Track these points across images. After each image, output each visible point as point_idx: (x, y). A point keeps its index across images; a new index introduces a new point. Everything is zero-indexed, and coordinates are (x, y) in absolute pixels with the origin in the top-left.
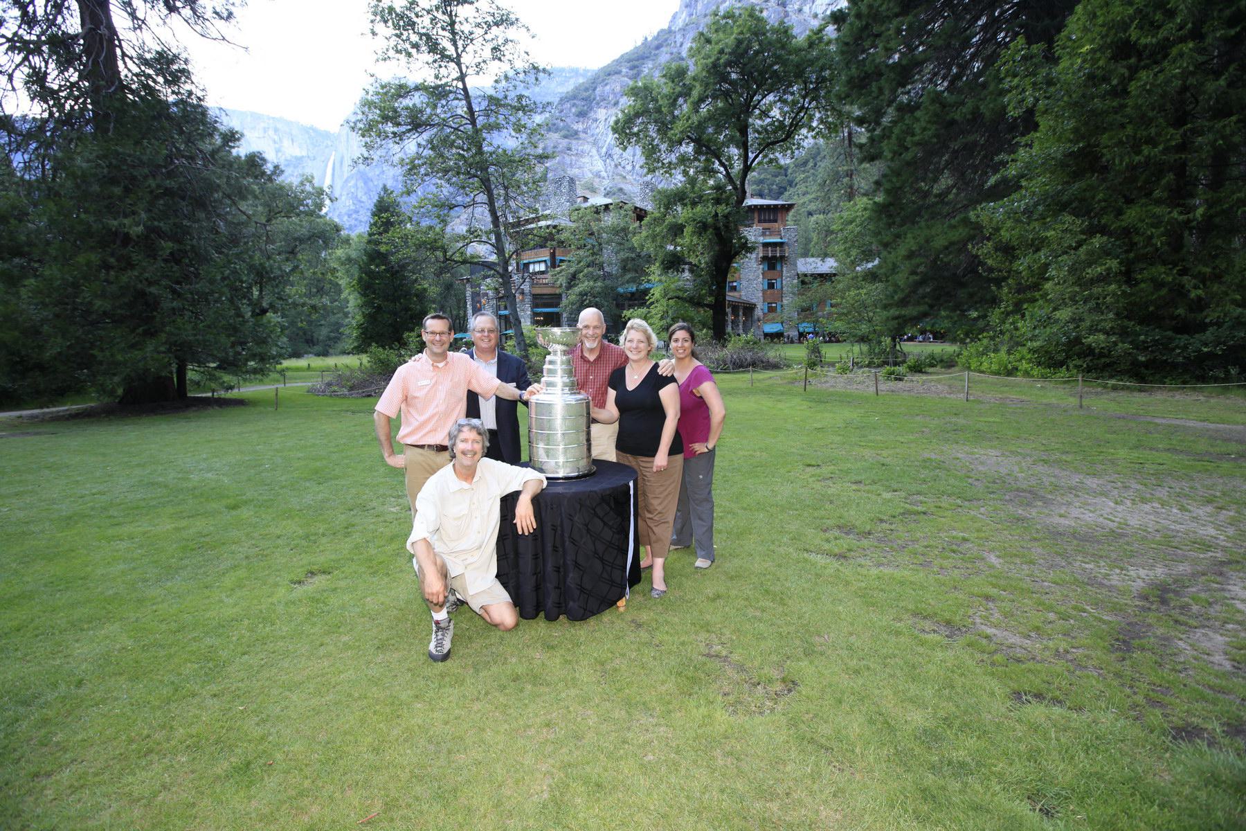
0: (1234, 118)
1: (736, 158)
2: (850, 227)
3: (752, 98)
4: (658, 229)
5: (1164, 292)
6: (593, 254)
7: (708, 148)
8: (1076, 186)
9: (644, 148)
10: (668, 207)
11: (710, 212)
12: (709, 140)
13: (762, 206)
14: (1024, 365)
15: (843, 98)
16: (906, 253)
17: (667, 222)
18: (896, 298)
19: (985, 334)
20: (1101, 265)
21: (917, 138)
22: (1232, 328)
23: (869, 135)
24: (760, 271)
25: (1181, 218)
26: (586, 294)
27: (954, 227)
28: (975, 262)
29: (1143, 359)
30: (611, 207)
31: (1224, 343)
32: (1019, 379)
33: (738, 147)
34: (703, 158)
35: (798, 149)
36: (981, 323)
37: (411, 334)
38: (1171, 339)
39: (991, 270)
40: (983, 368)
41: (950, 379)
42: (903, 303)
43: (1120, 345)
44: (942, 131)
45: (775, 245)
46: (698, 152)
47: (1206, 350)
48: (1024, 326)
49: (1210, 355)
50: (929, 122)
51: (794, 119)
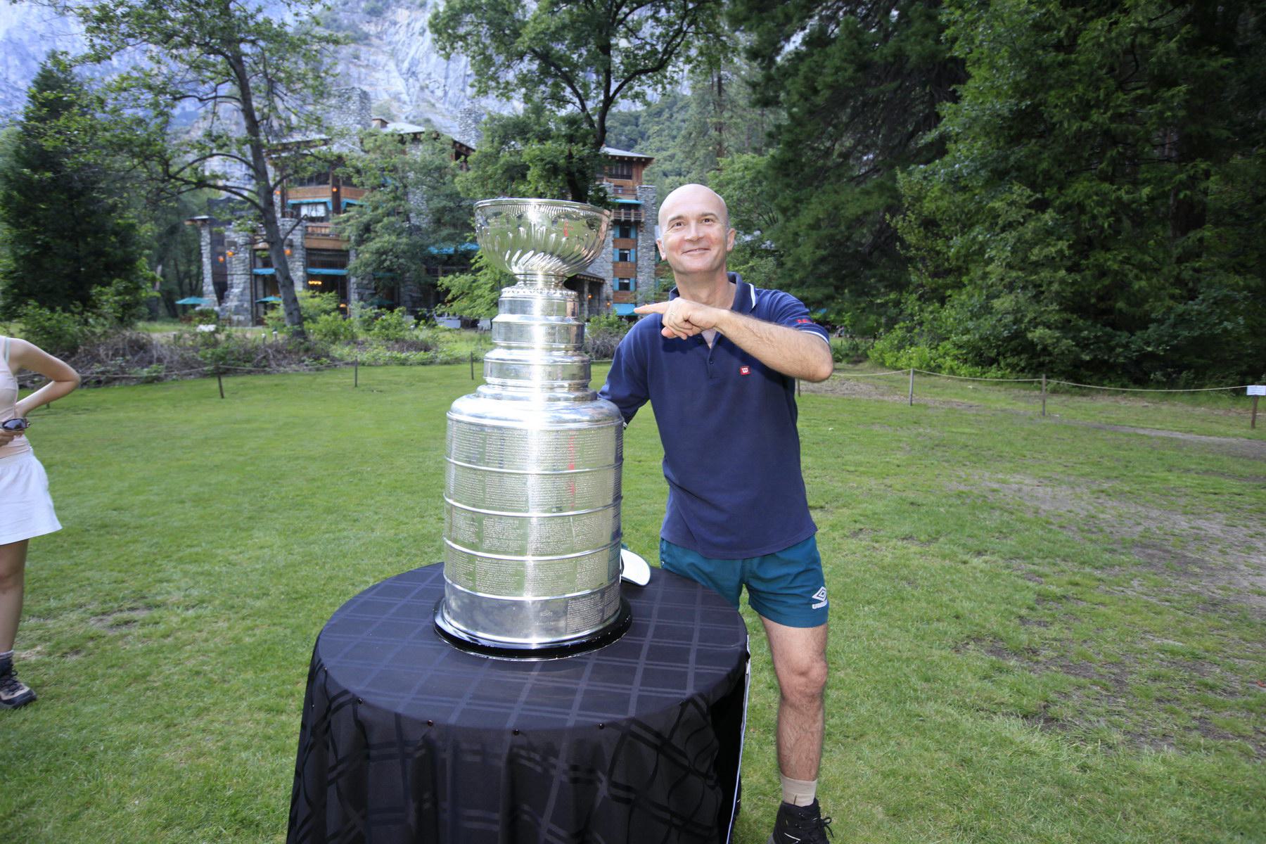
0: (1183, 88)
1: (593, 86)
3: (619, 7)
4: (490, 170)
5: (1107, 281)
6: (395, 198)
7: (558, 68)
8: (1019, 153)
10: (504, 141)
11: (563, 152)
12: (560, 58)
13: (614, 157)
14: (948, 362)
15: (736, 22)
16: (811, 222)
17: (502, 161)
18: (797, 277)
19: (902, 324)
20: (1049, 245)
21: (829, 79)
22: (1174, 326)
23: (764, 72)
24: (610, 239)
25: (1125, 197)
26: (385, 253)
27: (867, 193)
28: (887, 239)
29: (1088, 358)
30: (423, 136)
31: (1167, 343)
32: (943, 378)
33: (597, 73)
35: (670, 83)
36: (893, 311)
38: (1111, 337)
39: (906, 246)
40: (899, 365)
42: (802, 283)
43: (1065, 341)
46: (544, 72)
47: (1150, 349)
48: (949, 314)
49: (1152, 355)
50: (845, 60)
51: (669, 44)
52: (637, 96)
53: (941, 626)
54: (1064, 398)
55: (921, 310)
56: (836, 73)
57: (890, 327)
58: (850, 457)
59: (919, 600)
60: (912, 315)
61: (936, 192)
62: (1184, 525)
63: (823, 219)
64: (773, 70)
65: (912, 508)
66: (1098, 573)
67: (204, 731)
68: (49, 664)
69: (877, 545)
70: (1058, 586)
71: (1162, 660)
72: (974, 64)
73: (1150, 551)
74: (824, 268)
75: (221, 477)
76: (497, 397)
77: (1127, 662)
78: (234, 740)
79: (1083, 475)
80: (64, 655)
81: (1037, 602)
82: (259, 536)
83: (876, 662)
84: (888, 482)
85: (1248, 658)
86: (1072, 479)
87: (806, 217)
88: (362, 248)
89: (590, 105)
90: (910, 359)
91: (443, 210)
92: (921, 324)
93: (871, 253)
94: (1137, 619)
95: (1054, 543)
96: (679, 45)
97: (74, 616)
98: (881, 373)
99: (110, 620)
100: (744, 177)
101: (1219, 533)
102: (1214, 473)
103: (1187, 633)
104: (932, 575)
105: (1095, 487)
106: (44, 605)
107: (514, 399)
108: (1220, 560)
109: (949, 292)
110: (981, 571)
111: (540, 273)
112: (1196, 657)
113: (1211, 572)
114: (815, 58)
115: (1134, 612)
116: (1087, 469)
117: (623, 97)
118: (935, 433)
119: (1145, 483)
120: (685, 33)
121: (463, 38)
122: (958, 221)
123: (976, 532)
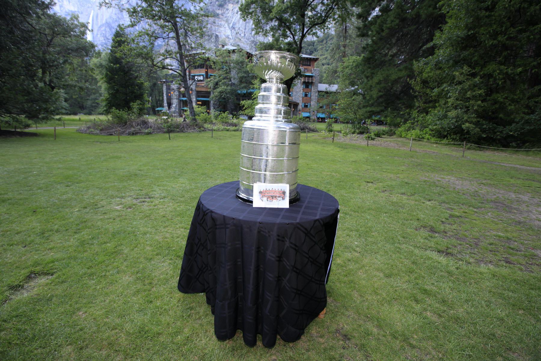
1: (298, 30)
2: (347, 70)
6: (226, 73)
9: (254, 21)
12: (286, 20)
15: (353, 5)
16: (377, 81)
18: (370, 103)
19: (410, 121)
21: (388, 26)
24: (302, 88)
26: (223, 92)
27: (401, 70)
30: (236, 51)
33: (300, 25)
34: (282, 29)
35: (327, 29)
36: (407, 116)
37: (135, 104)
41: (395, 141)
44: (401, 23)
45: (309, 76)
46: (280, 25)
50: (395, 18)
51: (327, 13)
52: (314, 34)
53: (411, 222)
54: (472, 151)
55: (418, 116)
56: (391, 23)
57: (405, 122)
58: (385, 167)
59: (404, 213)
60: (414, 118)
61: (428, 69)
62: (514, 196)
63: (382, 81)
64: (367, 23)
65: (406, 184)
66: (475, 210)
67: (166, 232)
68: (123, 211)
69: (391, 195)
70: (458, 213)
71: (495, 239)
72: (449, 17)
73: (497, 204)
74: (381, 100)
75: (170, 163)
76: (259, 120)
77: (481, 238)
78: (175, 235)
79: (475, 178)
80: (127, 209)
81: (450, 217)
82: (181, 180)
83: (386, 231)
84: (398, 175)
85: (530, 241)
86: (471, 179)
87: (376, 79)
88: (215, 91)
89: (296, 38)
90: (412, 135)
91: (242, 78)
92: (418, 121)
93: (400, 94)
94: (487, 225)
95: (459, 199)
96: (331, 13)
97: (129, 199)
98: (399, 139)
99: (139, 201)
100: (353, 65)
101: (527, 200)
102: (530, 180)
103: (507, 231)
104: (411, 206)
105: (479, 182)
106: (121, 195)
107: (264, 120)
108: (526, 209)
109: (430, 110)
110: (430, 206)
111: (275, 78)
112: (508, 239)
113: (521, 213)
114: (384, 17)
115: (487, 223)
116: (477, 176)
117: (309, 34)
118: (419, 161)
119: (500, 181)
120: (334, 8)
121: (251, 13)
122: (436, 81)
123: (429, 193)
